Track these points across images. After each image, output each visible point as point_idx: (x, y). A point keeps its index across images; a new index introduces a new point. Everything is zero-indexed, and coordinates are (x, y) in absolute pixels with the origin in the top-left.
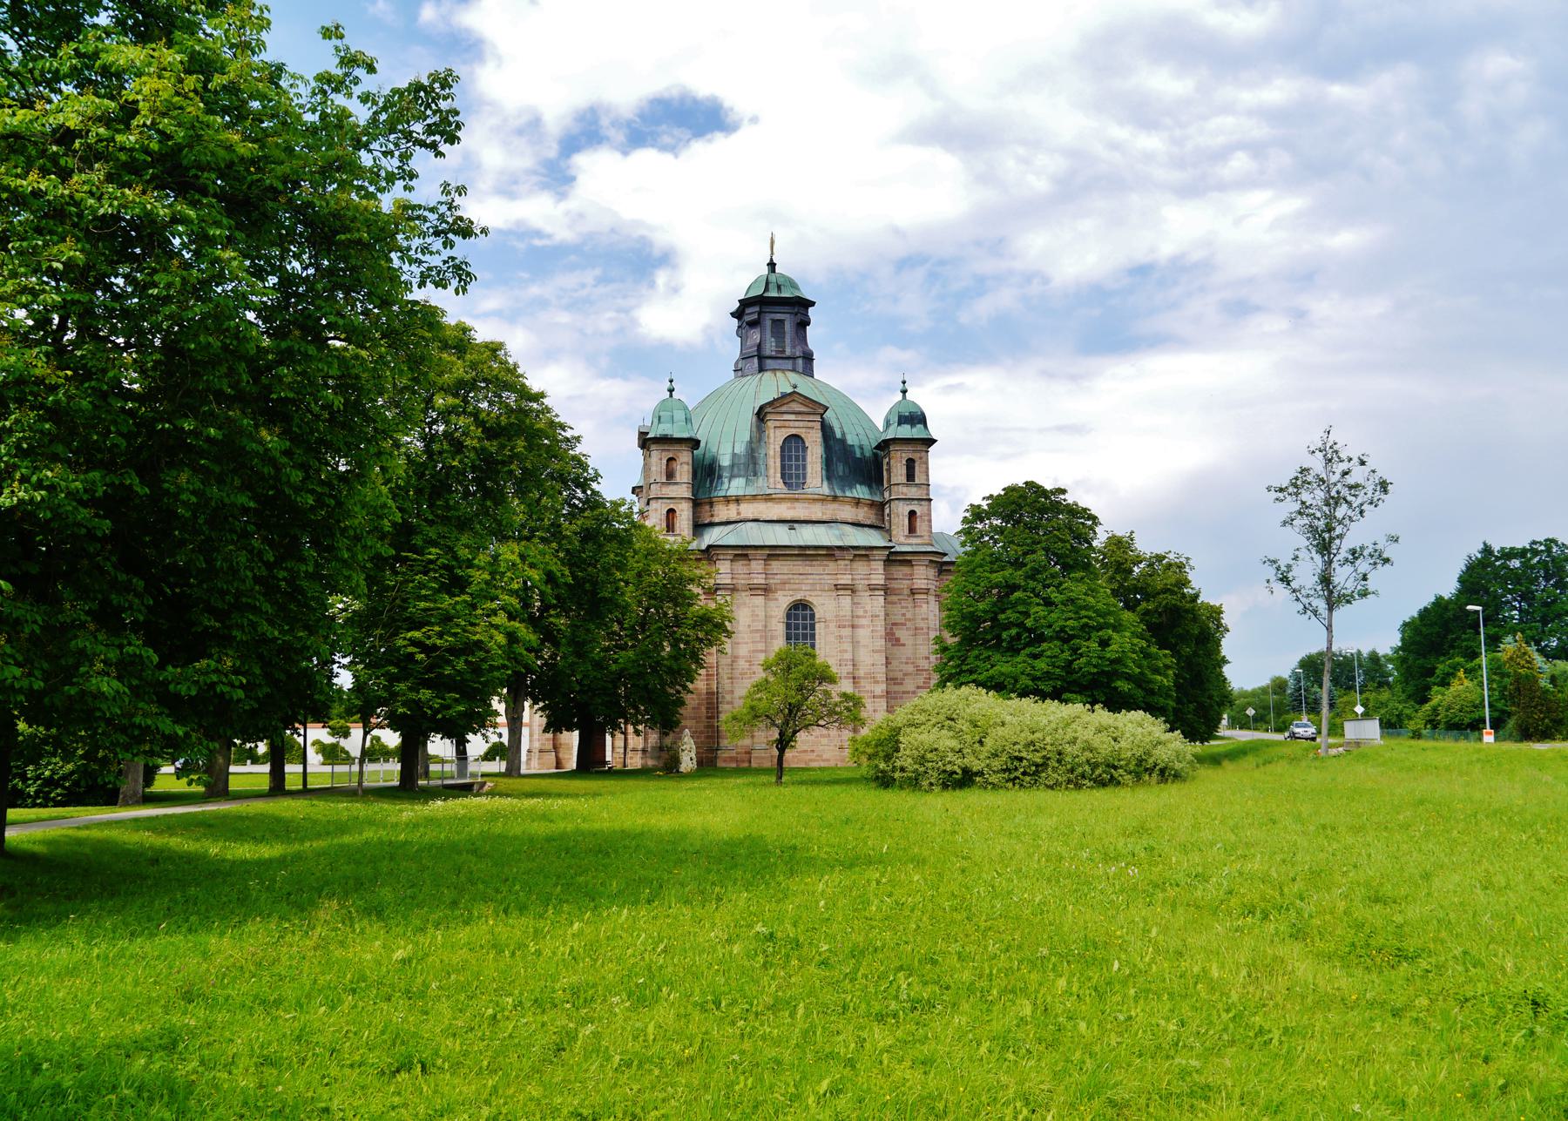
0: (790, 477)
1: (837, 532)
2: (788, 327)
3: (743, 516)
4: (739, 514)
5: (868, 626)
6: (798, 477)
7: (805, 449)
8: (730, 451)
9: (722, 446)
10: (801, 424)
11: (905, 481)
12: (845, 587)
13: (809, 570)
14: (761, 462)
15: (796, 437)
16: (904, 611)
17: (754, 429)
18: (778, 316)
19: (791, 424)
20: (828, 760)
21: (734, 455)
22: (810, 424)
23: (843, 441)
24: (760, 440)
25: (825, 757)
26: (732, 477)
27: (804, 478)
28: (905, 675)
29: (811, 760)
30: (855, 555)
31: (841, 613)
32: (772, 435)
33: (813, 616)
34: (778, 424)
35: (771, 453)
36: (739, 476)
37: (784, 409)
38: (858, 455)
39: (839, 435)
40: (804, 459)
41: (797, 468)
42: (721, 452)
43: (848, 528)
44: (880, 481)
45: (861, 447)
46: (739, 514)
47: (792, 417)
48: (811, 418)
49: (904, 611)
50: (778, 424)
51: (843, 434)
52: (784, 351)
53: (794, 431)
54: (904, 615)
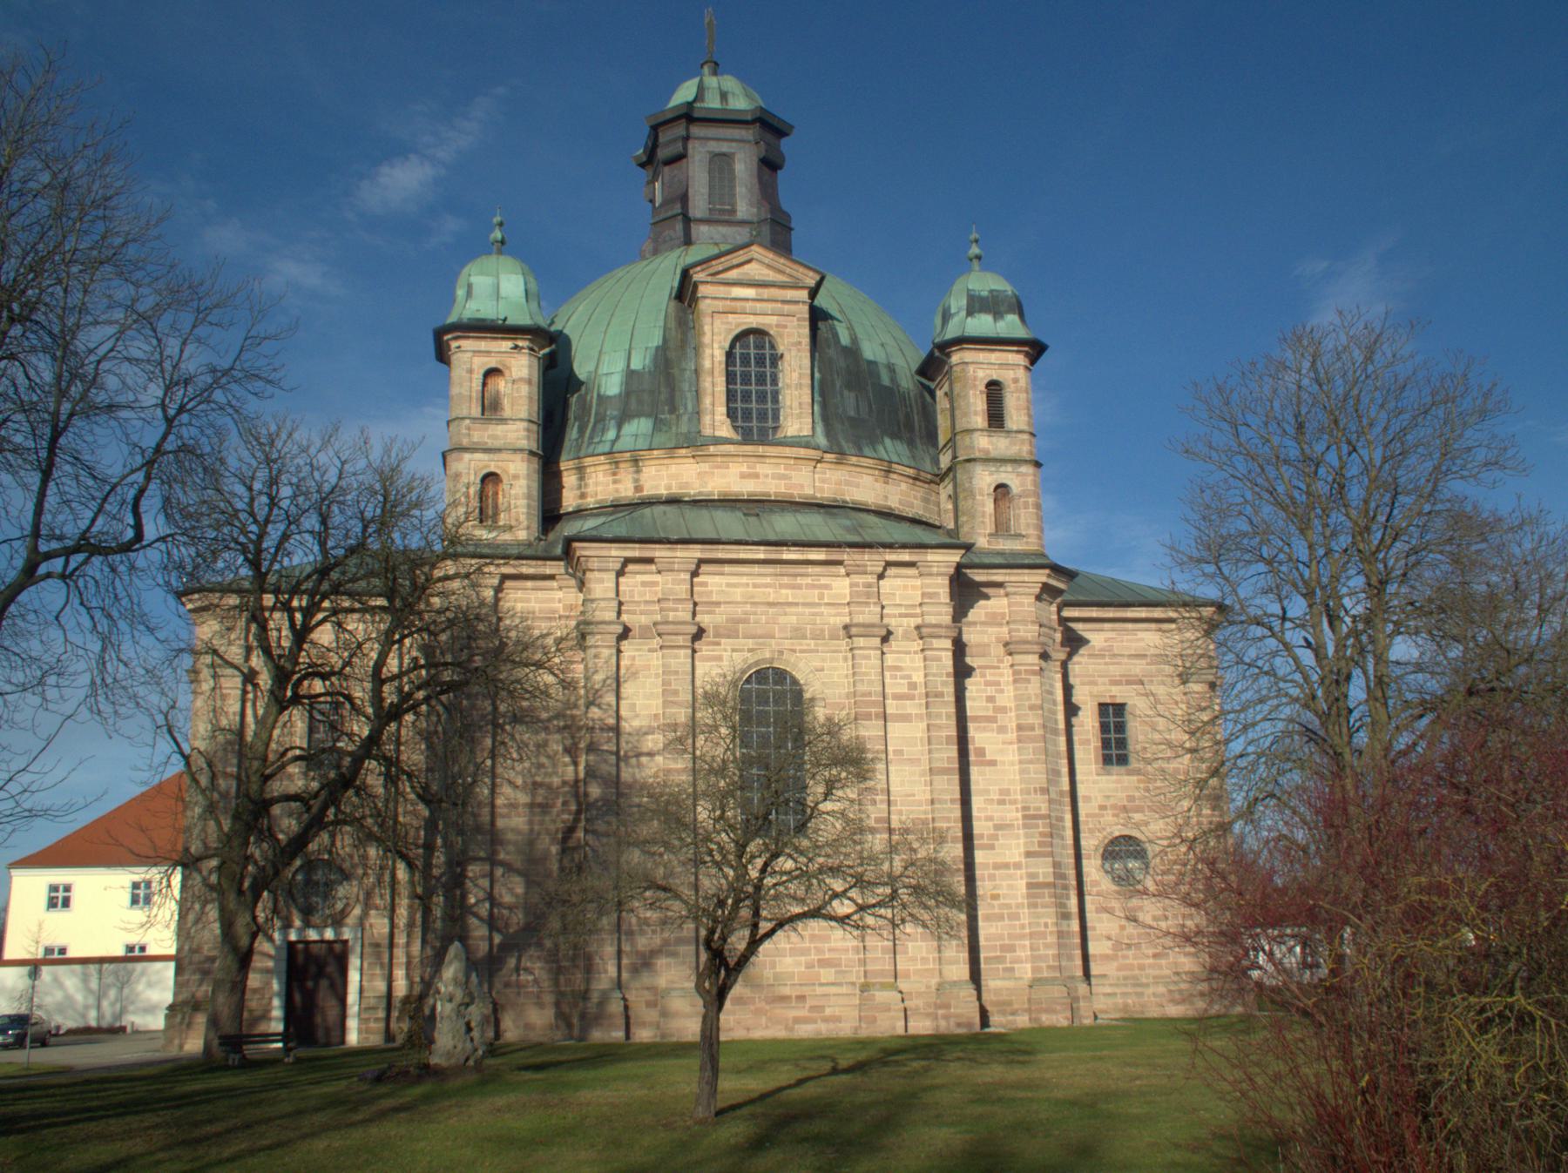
0: (747, 415)
1: (848, 523)
2: (744, 166)
3: (648, 491)
4: (638, 488)
5: (919, 717)
6: (763, 416)
7: (776, 359)
8: (620, 366)
9: (606, 358)
10: (769, 306)
11: (986, 424)
12: (867, 629)
13: (787, 594)
14: (686, 386)
15: (759, 333)
16: (990, 691)
17: (672, 324)
18: (724, 148)
19: (748, 305)
20: (837, 1019)
21: (630, 374)
22: (786, 307)
23: (853, 352)
24: (683, 344)
25: (828, 1011)
26: (622, 420)
27: (776, 417)
28: (998, 827)
29: (797, 1020)
30: (889, 564)
31: (861, 688)
32: (707, 328)
33: (798, 694)
34: (720, 305)
35: (707, 364)
36: (639, 415)
37: (733, 274)
38: (886, 380)
39: (845, 339)
40: (775, 381)
41: (762, 397)
42: (604, 369)
43: (872, 519)
44: (931, 435)
45: (891, 368)
46: (638, 488)
47: (750, 292)
48: (790, 294)
49: (990, 691)
50: (720, 305)
51: (854, 339)
52: (733, 211)
53: (752, 321)
54: (991, 699)
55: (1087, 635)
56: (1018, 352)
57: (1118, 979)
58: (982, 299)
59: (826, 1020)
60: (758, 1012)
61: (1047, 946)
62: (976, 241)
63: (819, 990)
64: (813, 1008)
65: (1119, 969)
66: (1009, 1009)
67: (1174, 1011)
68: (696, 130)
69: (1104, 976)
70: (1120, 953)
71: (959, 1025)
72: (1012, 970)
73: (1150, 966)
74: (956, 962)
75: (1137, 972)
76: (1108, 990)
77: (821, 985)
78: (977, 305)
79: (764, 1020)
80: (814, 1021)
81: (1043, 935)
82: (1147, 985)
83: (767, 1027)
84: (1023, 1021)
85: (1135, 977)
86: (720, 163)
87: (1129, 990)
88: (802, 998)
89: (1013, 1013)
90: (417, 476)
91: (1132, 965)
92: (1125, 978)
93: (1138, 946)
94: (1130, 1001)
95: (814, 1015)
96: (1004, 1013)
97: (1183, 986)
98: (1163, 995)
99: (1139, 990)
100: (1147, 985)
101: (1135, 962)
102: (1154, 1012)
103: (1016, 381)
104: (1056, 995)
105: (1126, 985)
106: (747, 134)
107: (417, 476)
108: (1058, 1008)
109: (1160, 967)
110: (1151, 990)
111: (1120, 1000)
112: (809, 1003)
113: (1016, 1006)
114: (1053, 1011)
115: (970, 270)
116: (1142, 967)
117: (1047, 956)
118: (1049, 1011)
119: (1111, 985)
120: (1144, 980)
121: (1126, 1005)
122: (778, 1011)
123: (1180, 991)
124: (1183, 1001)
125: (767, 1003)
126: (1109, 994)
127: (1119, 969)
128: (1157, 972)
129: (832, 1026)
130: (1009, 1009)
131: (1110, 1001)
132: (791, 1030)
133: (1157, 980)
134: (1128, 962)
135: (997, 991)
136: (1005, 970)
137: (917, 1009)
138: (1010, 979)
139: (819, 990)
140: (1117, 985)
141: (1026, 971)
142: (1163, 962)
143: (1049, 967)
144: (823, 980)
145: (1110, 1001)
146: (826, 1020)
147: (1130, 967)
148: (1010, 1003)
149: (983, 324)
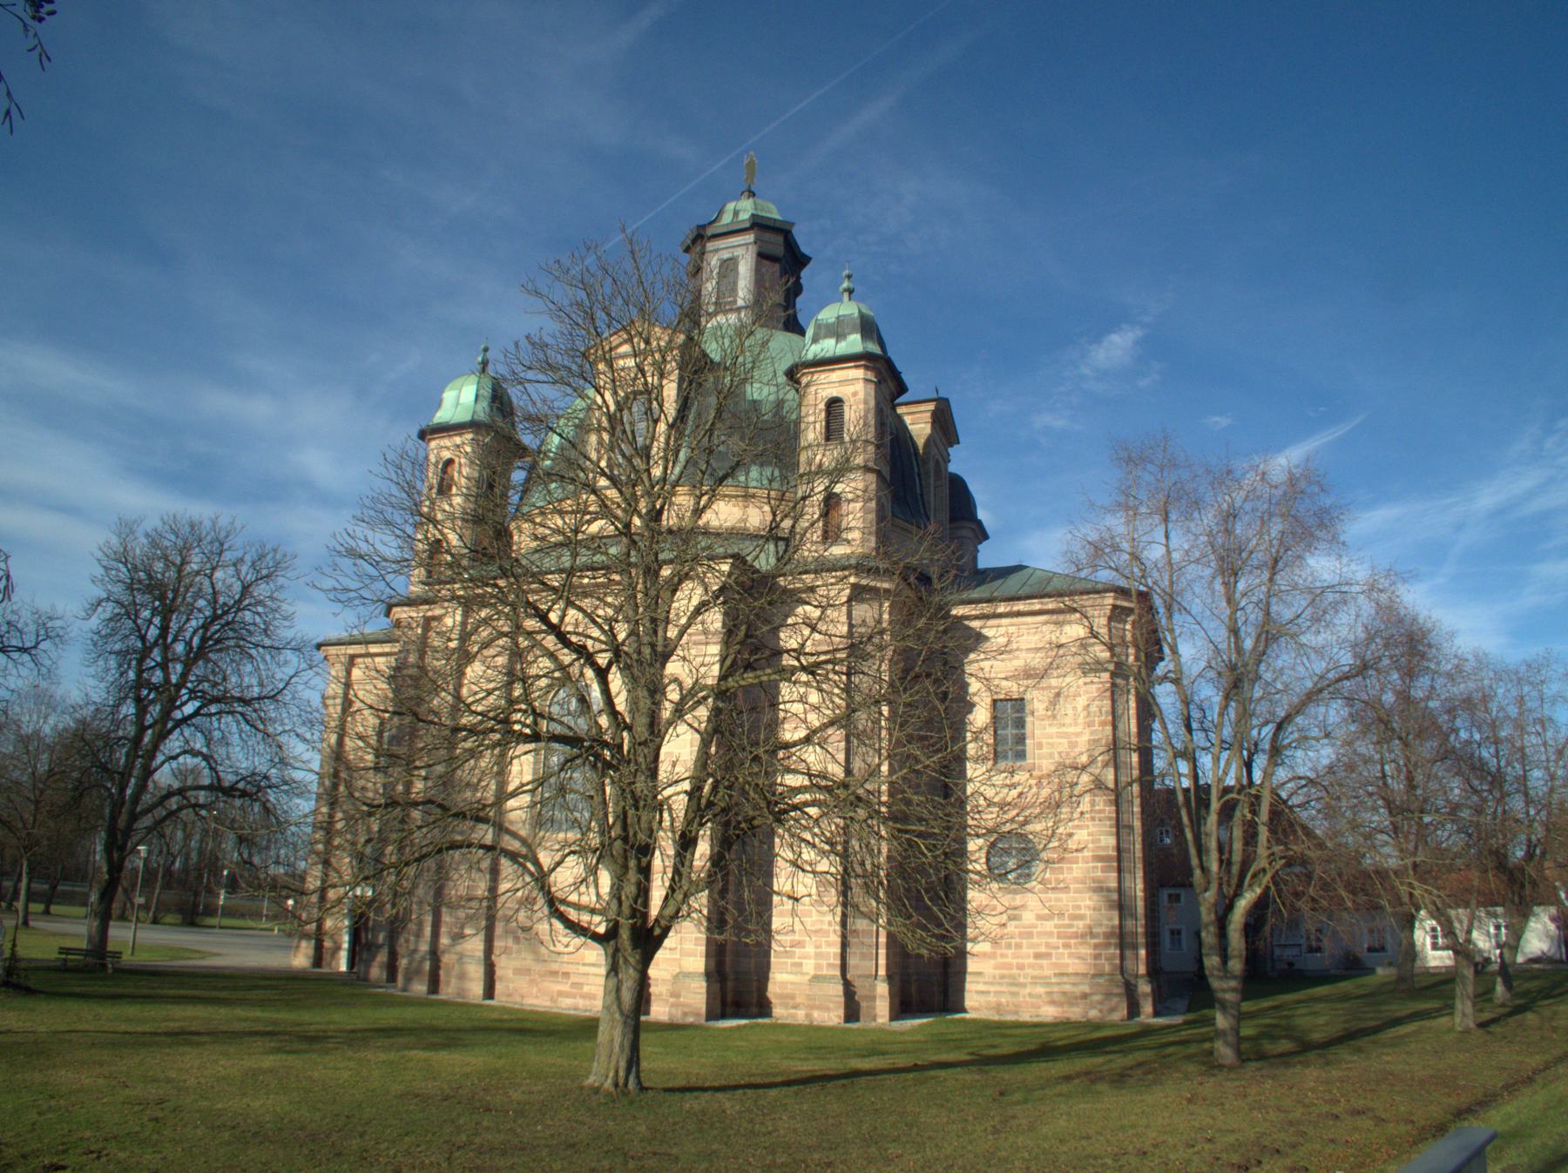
25: (586, 989)
29: (560, 994)
55: (985, 632)
56: (856, 367)
57: (994, 977)
58: (828, 326)
59: (583, 996)
60: (532, 982)
61: (829, 944)
62: (849, 277)
63: (583, 969)
64: (574, 985)
65: (996, 967)
66: (791, 1002)
67: (1049, 1013)
68: (710, 246)
69: (979, 974)
70: (999, 952)
71: (685, 1014)
72: (800, 965)
73: (1032, 966)
74: (692, 954)
75: (1015, 971)
76: (981, 987)
77: (584, 964)
78: (823, 332)
79: (535, 990)
80: (574, 996)
81: (826, 933)
82: (1023, 985)
83: (537, 997)
84: (800, 1016)
85: (1012, 977)
86: (729, 266)
87: (1004, 989)
88: (566, 975)
89: (795, 1007)
90: (269, 547)
91: (1011, 964)
92: (1002, 977)
93: (1018, 946)
94: (1003, 1000)
95: (575, 991)
96: (786, 1006)
97: (1068, 988)
98: (1040, 996)
99: (1014, 989)
100: (1023, 985)
101: (1015, 961)
102: (1026, 1017)
103: (855, 394)
104: (831, 993)
105: (999, 984)
106: (750, 238)
107: (269, 547)
108: (831, 1005)
109: (1041, 967)
110: (1028, 990)
111: (992, 999)
112: (573, 979)
113: (798, 1000)
114: (828, 1009)
115: (840, 300)
116: (1021, 967)
117: (828, 953)
118: (819, 1008)
119: (985, 983)
120: (1022, 980)
121: (999, 1005)
122: (546, 984)
123: (1064, 993)
124: (1060, 1004)
125: (541, 976)
126: (983, 992)
127: (996, 967)
128: (1036, 973)
129: (587, 1002)
130: (791, 1002)
131: (982, 999)
132: (556, 1001)
133: (1036, 980)
134: (1006, 960)
135: (783, 984)
136: (794, 964)
137: (661, 994)
138: (796, 973)
139: (583, 969)
140: (991, 984)
141: (809, 967)
142: (1044, 962)
143: (829, 965)
144: (587, 961)
145: (982, 999)
146: (583, 996)
147: (1009, 966)
148: (793, 997)
149: (828, 347)
